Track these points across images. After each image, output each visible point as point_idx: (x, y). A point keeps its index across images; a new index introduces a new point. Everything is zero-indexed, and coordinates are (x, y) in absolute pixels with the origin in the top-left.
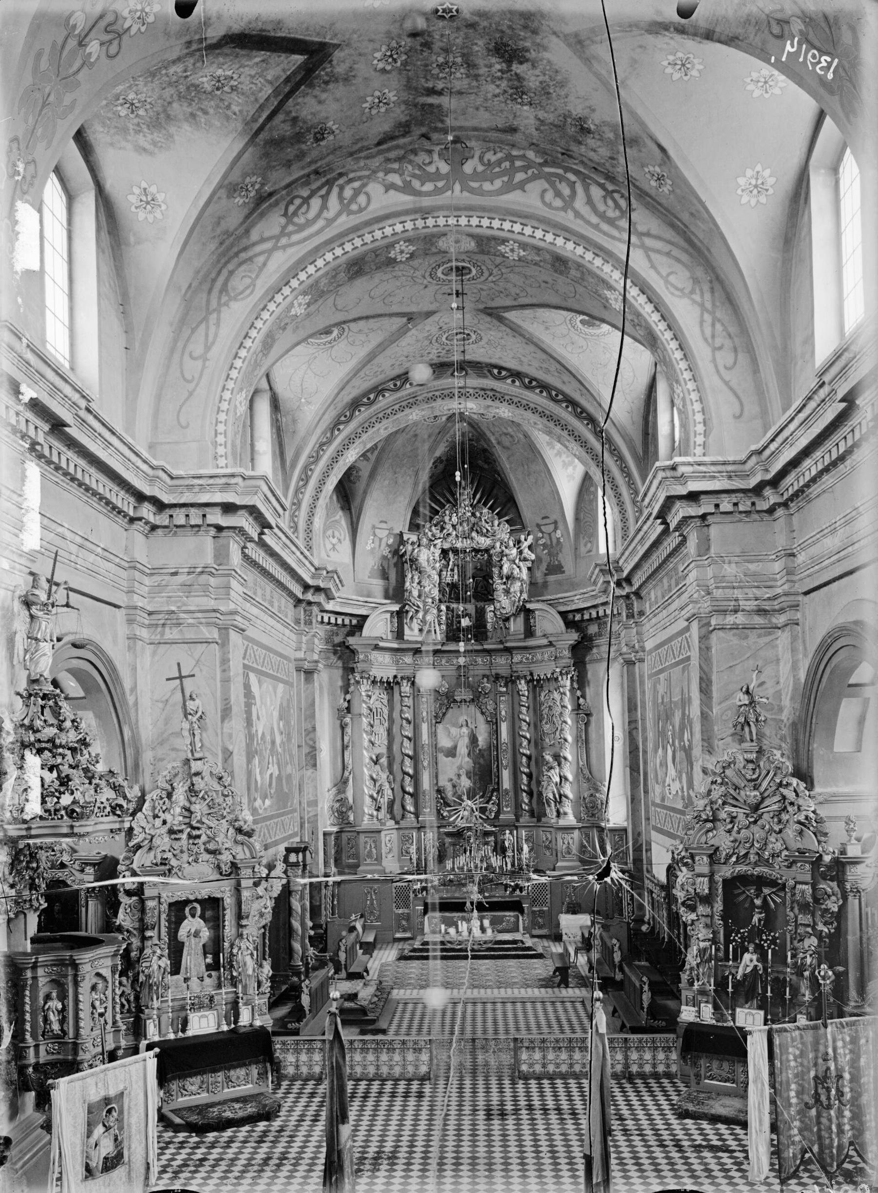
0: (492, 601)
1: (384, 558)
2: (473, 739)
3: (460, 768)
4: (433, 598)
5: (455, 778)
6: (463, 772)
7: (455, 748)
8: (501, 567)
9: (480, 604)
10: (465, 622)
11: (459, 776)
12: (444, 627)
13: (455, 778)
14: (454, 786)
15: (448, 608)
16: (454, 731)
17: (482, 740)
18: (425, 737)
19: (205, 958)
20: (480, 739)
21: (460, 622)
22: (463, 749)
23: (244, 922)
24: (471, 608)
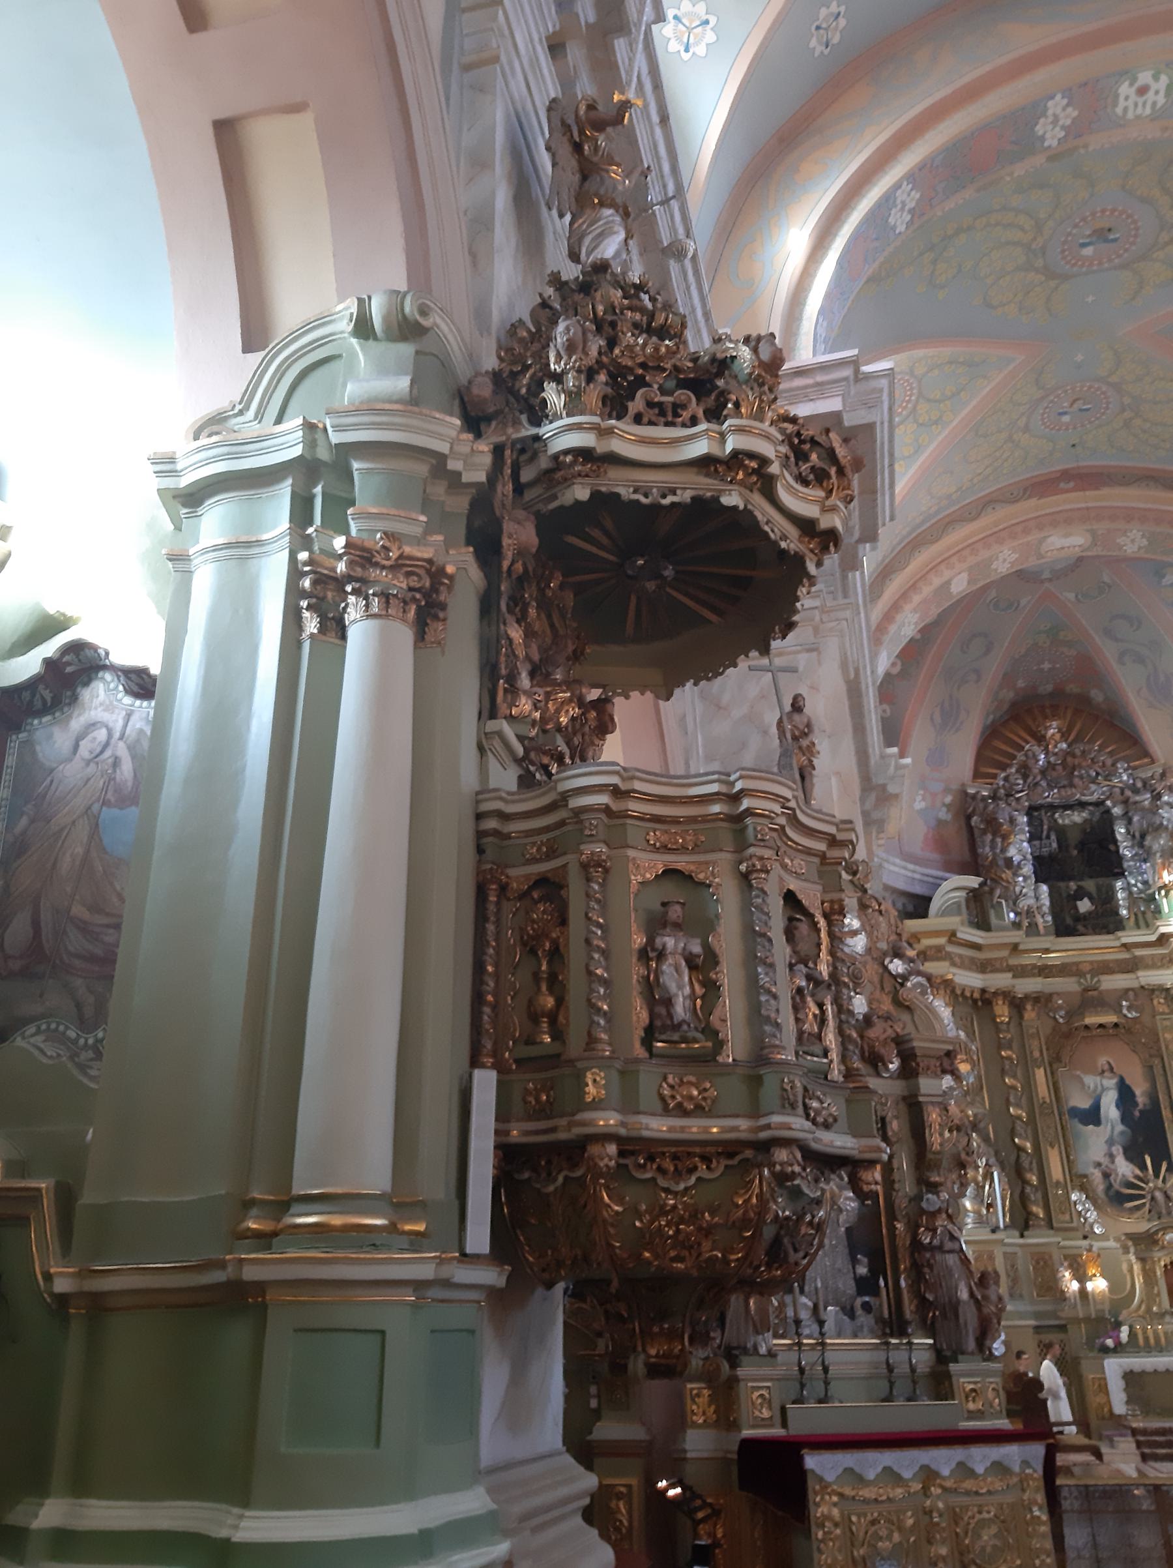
0: (1121, 874)
1: (940, 823)
2: (1125, 1095)
3: (1110, 1142)
4: (1026, 878)
5: (1105, 1161)
6: (1118, 1150)
7: (1096, 1108)
8: (1130, 822)
9: (1101, 881)
10: (1084, 906)
11: (1112, 1157)
12: (1049, 918)
13: (1105, 1161)
14: (1106, 1176)
15: (1050, 888)
16: (1090, 1081)
17: (1140, 1091)
18: (1042, 1089)
19: (854, 1262)
20: (1138, 1092)
21: (1076, 908)
22: (1110, 1110)
23: (935, 1178)
24: (1090, 885)
